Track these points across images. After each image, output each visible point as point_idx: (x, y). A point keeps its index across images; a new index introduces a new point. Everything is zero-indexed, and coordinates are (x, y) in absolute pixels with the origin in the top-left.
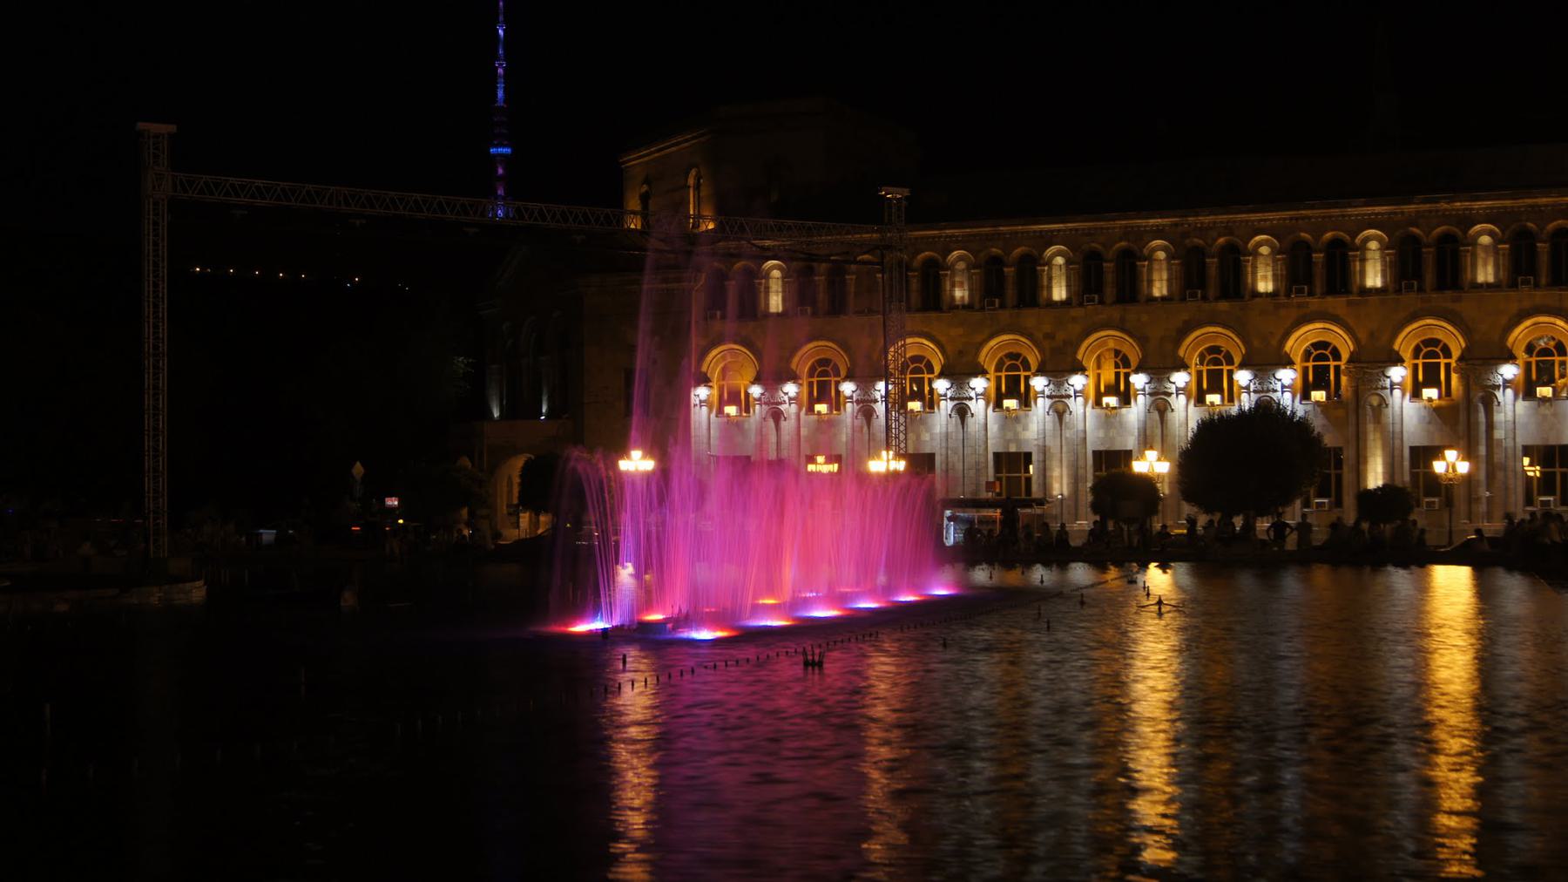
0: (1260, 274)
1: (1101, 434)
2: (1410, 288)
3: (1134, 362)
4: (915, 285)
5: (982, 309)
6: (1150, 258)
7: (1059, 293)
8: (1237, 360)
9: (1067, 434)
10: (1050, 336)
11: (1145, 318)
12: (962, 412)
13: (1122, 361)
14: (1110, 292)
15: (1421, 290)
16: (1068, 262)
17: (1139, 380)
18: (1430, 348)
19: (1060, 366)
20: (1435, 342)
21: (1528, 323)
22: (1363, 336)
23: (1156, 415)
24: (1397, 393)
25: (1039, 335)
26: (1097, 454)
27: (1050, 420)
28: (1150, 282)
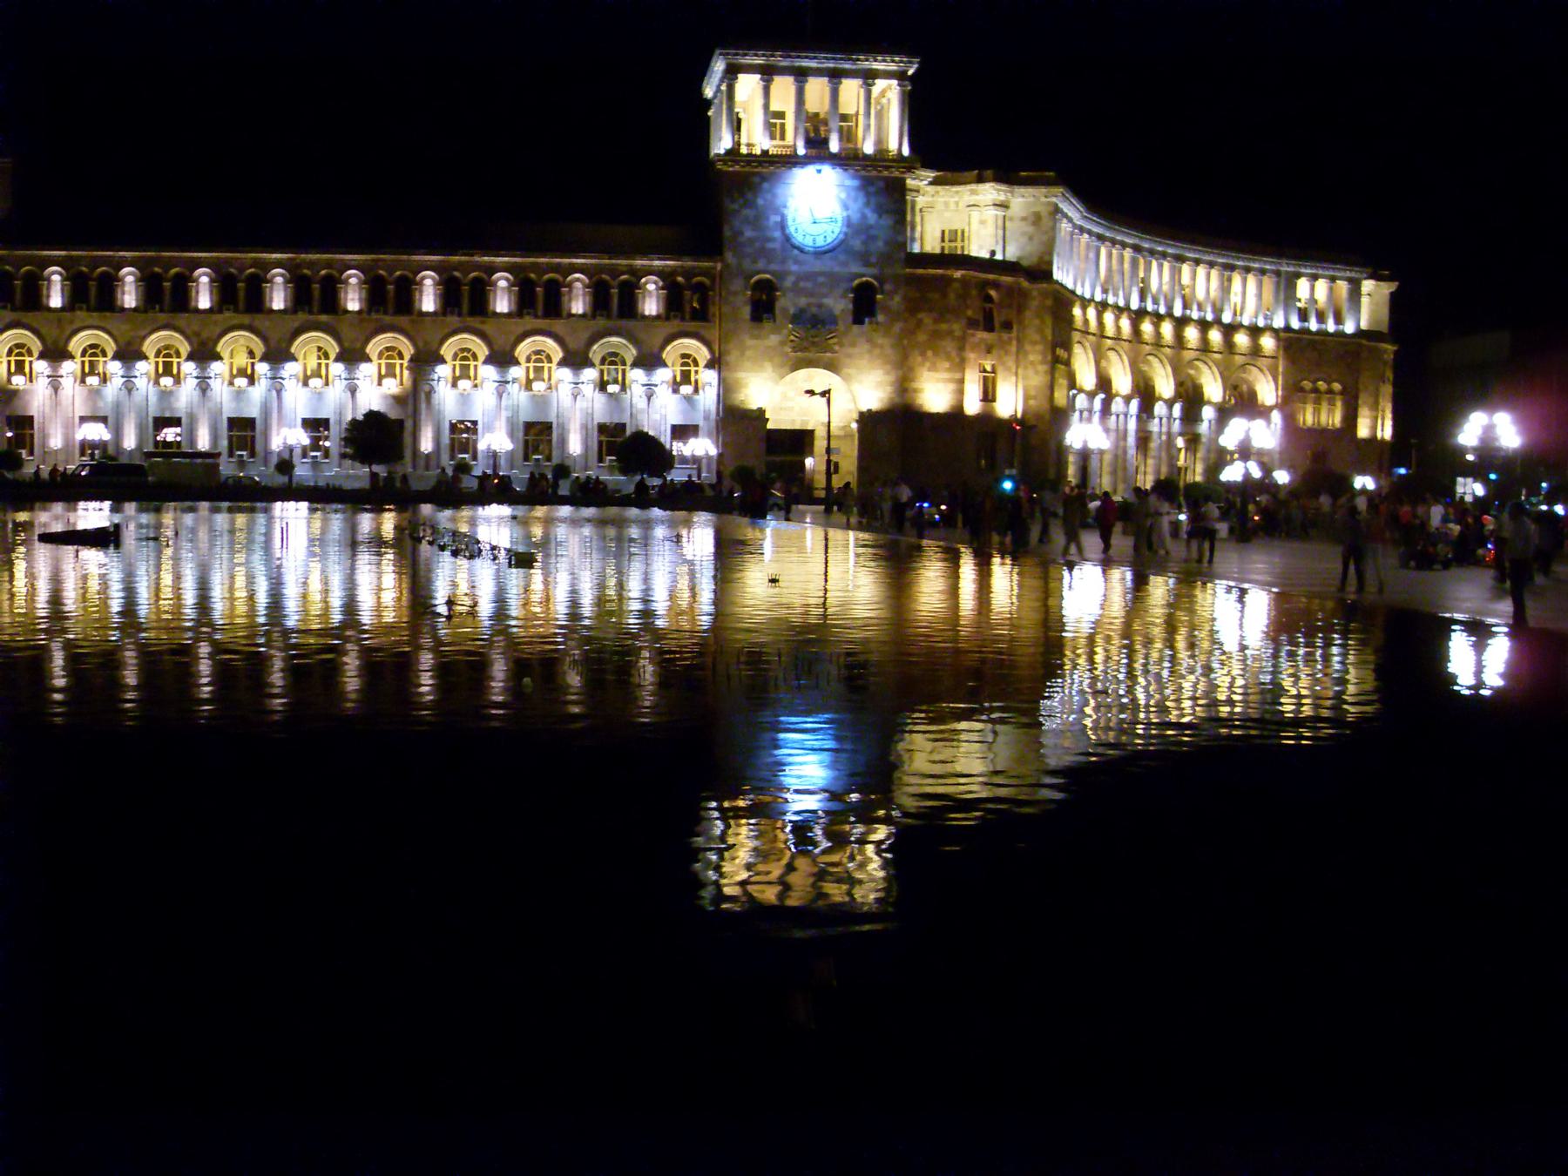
0: (350, 296)
1: (233, 405)
2: (452, 313)
3: (258, 354)
4: (93, 292)
5: (146, 311)
6: (270, 281)
7: (204, 302)
8: (332, 356)
9: (210, 405)
10: (197, 334)
11: (267, 323)
12: (129, 387)
13: (251, 354)
14: (241, 305)
15: (460, 315)
16: (212, 281)
17: (262, 368)
18: (465, 355)
19: (55, 353)
20: (468, 350)
21: (529, 340)
22: (421, 344)
23: (274, 393)
24: (442, 383)
25: (189, 332)
26: (230, 420)
27: (196, 393)
28: (271, 300)
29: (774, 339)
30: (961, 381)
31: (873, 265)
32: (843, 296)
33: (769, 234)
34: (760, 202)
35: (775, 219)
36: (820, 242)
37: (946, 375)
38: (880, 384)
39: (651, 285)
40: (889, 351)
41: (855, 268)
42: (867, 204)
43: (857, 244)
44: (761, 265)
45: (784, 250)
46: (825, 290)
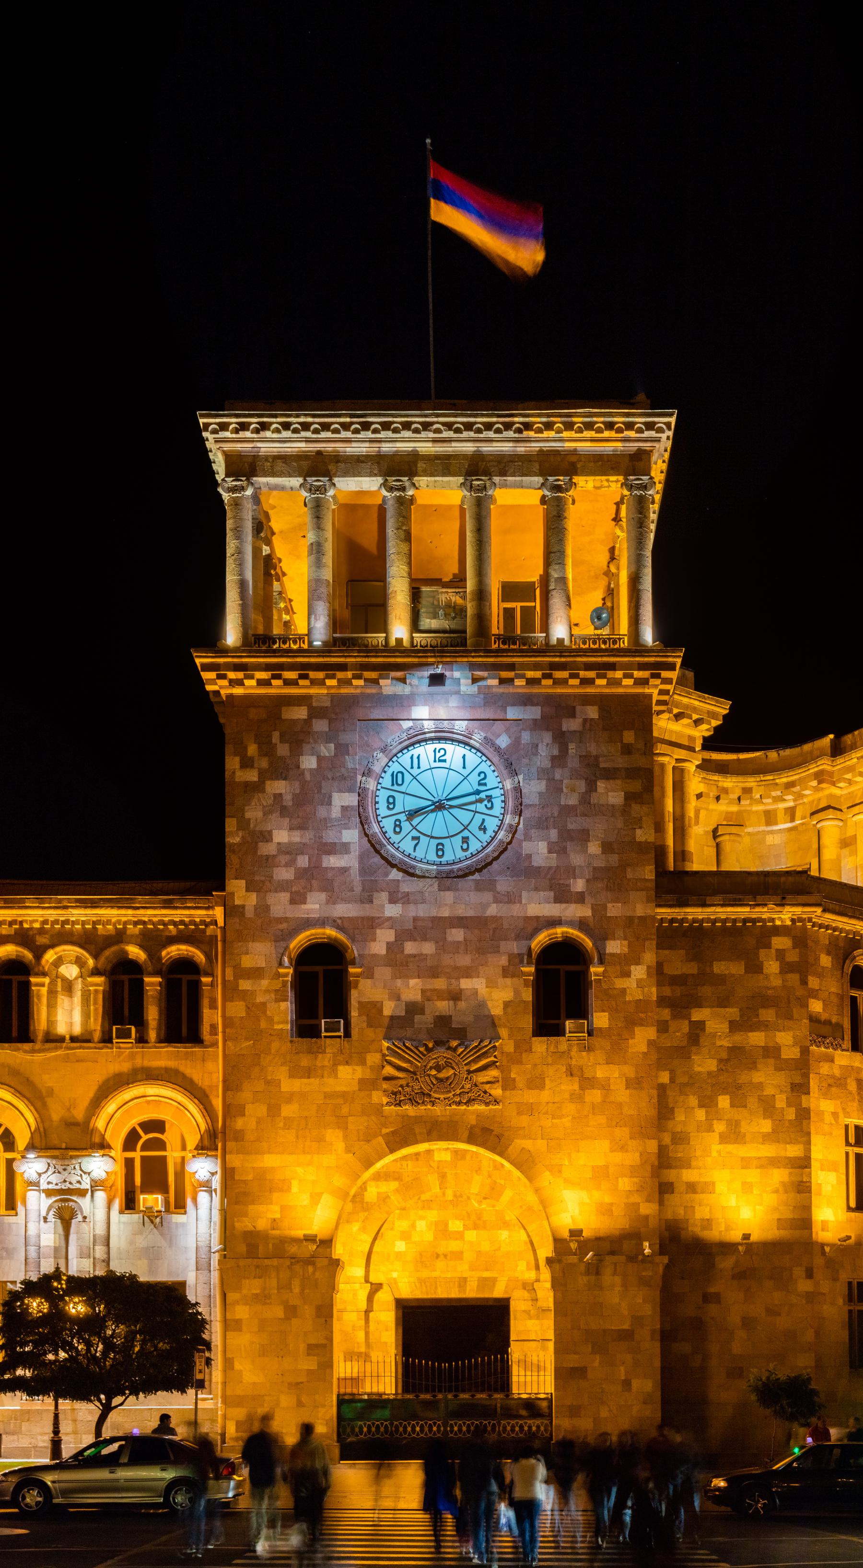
29: (348, 1076)
30: (804, 1163)
31: (580, 898)
32: (506, 973)
33: (330, 836)
34: (309, 762)
35: (351, 799)
36: (453, 852)
37: (767, 1151)
38: (601, 1174)
39: (68, 964)
40: (621, 1094)
41: (538, 906)
42: (559, 760)
43: (539, 851)
44: (314, 905)
45: (364, 870)
46: (464, 960)
